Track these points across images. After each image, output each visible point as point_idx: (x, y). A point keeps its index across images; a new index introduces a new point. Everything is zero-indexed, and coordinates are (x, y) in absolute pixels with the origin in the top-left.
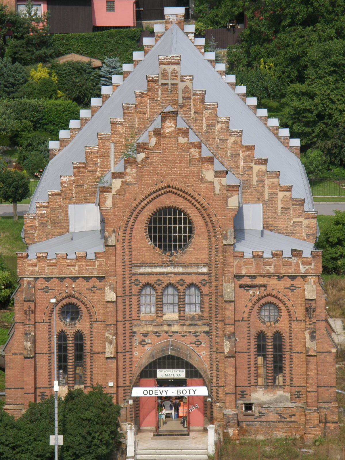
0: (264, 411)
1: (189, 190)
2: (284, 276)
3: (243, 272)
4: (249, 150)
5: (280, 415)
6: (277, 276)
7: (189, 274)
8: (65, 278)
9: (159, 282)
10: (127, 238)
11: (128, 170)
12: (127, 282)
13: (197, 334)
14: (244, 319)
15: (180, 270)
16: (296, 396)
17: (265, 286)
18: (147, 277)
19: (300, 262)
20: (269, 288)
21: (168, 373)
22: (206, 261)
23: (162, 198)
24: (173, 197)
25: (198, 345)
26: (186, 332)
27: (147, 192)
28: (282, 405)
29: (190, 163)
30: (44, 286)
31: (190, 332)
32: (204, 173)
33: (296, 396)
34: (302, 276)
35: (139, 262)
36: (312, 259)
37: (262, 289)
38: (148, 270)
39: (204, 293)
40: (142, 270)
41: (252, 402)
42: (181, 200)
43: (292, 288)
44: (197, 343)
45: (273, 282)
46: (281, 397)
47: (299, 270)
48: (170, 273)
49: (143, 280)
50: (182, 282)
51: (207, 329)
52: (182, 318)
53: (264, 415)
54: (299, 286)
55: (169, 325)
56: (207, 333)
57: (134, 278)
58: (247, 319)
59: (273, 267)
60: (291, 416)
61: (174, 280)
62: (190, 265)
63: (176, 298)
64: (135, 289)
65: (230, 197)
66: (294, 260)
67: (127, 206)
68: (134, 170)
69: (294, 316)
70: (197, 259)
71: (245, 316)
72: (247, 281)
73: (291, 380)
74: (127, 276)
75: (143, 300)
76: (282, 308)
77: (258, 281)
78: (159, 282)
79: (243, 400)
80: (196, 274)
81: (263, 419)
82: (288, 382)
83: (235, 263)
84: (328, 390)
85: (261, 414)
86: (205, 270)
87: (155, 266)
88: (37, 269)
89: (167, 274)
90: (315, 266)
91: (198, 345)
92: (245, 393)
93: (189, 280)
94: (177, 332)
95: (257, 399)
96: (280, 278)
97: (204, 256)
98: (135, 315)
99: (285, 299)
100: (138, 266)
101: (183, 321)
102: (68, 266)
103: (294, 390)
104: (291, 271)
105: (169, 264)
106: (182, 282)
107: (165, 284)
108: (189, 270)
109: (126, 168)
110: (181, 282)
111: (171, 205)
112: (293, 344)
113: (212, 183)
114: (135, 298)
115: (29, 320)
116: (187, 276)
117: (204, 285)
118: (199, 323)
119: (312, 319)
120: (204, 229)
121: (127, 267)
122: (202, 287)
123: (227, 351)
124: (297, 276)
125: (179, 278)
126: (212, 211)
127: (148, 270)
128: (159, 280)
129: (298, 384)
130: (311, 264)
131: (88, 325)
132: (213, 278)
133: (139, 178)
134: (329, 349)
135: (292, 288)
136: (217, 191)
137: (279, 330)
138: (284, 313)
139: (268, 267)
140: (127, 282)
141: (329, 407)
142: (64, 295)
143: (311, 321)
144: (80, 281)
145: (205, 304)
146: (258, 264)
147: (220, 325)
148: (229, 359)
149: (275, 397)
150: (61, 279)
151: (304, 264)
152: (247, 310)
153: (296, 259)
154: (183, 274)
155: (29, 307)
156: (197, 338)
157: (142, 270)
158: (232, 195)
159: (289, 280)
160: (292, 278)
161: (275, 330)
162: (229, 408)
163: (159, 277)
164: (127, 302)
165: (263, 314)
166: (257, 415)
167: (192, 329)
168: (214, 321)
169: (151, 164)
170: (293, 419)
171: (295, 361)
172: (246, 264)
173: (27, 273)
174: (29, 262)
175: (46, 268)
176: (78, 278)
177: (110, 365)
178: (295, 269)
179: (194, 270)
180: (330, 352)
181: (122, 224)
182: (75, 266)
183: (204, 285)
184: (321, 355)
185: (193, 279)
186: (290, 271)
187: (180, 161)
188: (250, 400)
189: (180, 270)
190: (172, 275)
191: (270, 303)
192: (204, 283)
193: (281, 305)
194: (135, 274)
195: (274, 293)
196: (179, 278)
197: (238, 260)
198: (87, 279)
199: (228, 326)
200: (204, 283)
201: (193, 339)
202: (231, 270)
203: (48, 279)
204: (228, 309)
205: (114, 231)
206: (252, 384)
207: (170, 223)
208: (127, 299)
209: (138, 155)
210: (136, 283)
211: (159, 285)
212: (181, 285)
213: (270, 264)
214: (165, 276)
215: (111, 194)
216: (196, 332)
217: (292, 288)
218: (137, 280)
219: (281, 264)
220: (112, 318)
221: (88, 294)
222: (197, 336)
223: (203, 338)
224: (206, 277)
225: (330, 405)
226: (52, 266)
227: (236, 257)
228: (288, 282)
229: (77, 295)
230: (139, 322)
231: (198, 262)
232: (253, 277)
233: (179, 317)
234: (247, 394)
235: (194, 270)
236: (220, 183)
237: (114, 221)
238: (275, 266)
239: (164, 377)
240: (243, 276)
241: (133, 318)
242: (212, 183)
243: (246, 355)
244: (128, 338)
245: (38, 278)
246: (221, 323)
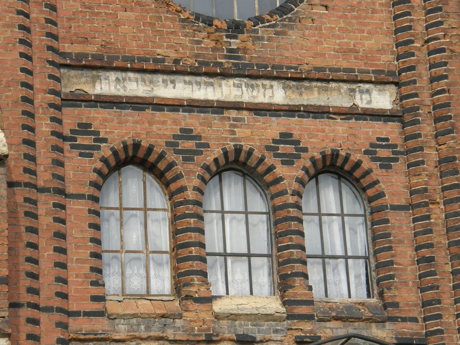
9: (190, 145)
12: (44, 126)
15: (277, 94)
18: (130, 115)
22: (387, 60)
35: (91, 49)
38: (135, 87)
40: (107, 85)
48: (237, 106)
49: (118, 130)
50: (289, 149)
57: (71, 117)
62: (324, 78)
64: (79, 170)
70: (346, 52)
78: (190, 145)
86: (383, 99)
89: (220, 107)
97: (376, 43)
105: (227, 63)
106: (289, 149)
107: (216, 152)
108: (314, 97)
116: (308, 122)
117: (386, 164)
122: (378, 173)
125: (275, 127)
127: (135, 87)
128: (187, 134)
132: (427, 129)
140: (44, 126)
145: (399, 249)
154: (291, 111)
157: (107, 85)
179: (337, 97)
189: (277, 94)
190: (245, 114)
196: (275, 127)
210: (81, 140)
211: (189, 156)
212: (288, 160)
214: (214, 119)
224: (391, 131)
235: (337, 97)
241: (73, 307)
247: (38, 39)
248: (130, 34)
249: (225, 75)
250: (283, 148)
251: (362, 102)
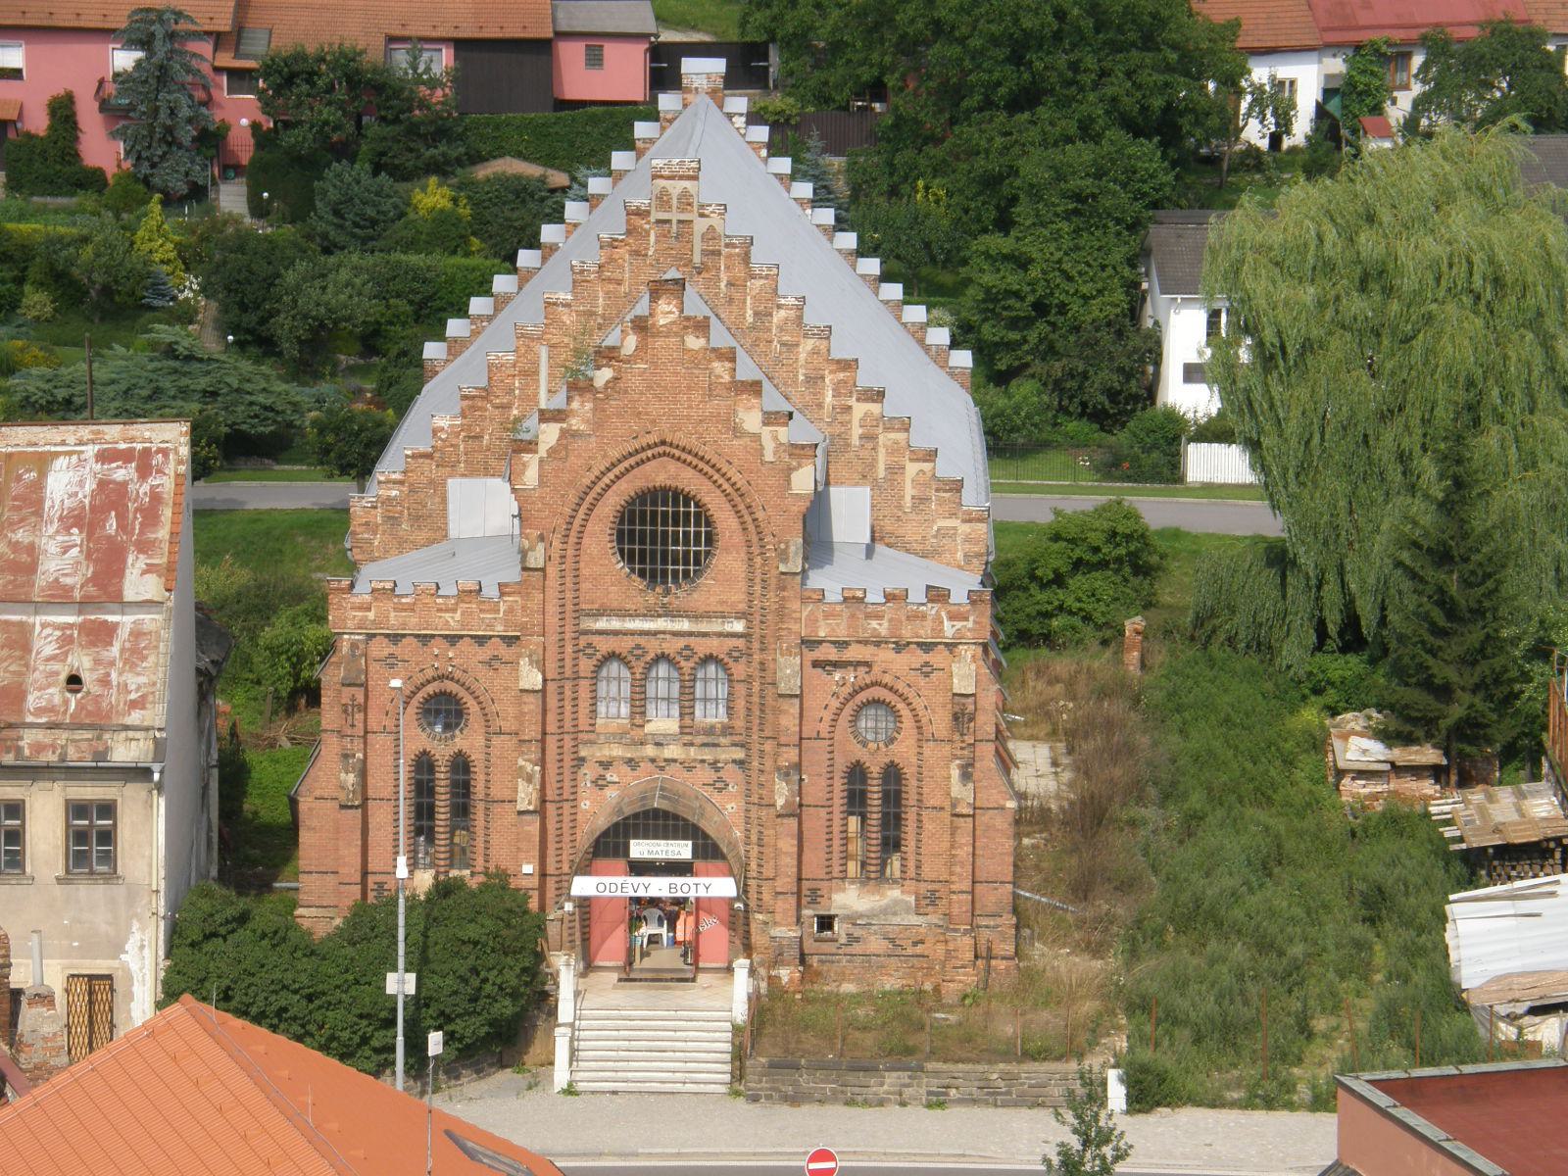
0: (857, 932)
1: (708, 452)
2: (909, 643)
3: (822, 634)
4: (844, 370)
5: (892, 941)
7: (705, 635)
8: (433, 636)
9: (640, 652)
10: (570, 552)
11: (575, 405)
12: (569, 649)
14: (822, 735)
15: (684, 625)
16: (928, 901)
17: (867, 664)
19: (943, 614)
20: (876, 669)
22: (742, 607)
23: (648, 467)
24: (673, 467)
25: (720, 790)
26: (695, 760)
27: (615, 454)
28: (897, 920)
29: (710, 392)
30: (386, 653)
31: (703, 761)
32: (740, 415)
33: (928, 901)
34: (946, 645)
35: (596, 606)
36: (969, 607)
37: (862, 670)
38: (615, 624)
39: (735, 677)
40: (602, 624)
41: (832, 912)
42: (689, 473)
44: (718, 785)
45: (885, 656)
46: (896, 902)
47: (942, 630)
48: (664, 632)
49: (604, 645)
51: (740, 754)
53: (857, 940)
54: (941, 666)
55: (658, 744)
56: (740, 763)
57: (583, 641)
58: (827, 736)
59: (885, 624)
60: (915, 944)
61: (672, 646)
62: (707, 616)
63: (676, 687)
64: (586, 665)
65: (796, 469)
66: (932, 610)
67: (571, 483)
68: (589, 406)
69: (928, 730)
70: (722, 603)
71: (824, 728)
72: (830, 653)
73: (918, 867)
74: (568, 636)
75: (602, 687)
76: (902, 713)
77: (854, 653)
78: (640, 652)
80: (720, 635)
81: (857, 948)
82: (911, 872)
83: (804, 614)
85: (853, 939)
86: (739, 626)
87: (631, 616)
88: (371, 615)
89: (655, 633)
90: (975, 622)
91: (720, 790)
93: (703, 647)
95: (844, 907)
96: (900, 647)
97: (737, 597)
98: (583, 722)
99: (911, 694)
100: (594, 615)
101: (689, 737)
102: (440, 610)
103: (923, 887)
104: (925, 634)
107: (652, 655)
109: (569, 399)
110: (685, 653)
111: (668, 483)
112: (925, 790)
113: (757, 437)
114: (584, 684)
115: (353, 726)
117: (736, 659)
118: (723, 740)
120: (739, 538)
121: (569, 615)
122: (731, 664)
123: (780, 802)
124: (936, 644)
125: (681, 642)
126: (757, 500)
127: (615, 624)
128: (638, 647)
129: (933, 876)
130: (966, 619)
131: (480, 741)
132: (756, 645)
133: (598, 423)
134: (1002, 802)
135: (926, 670)
136: (769, 456)
137: (896, 761)
139: (874, 624)
140: (569, 649)
141: (997, 926)
142: (430, 673)
144: (464, 645)
146: (853, 616)
147: (768, 746)
148: (785, 821)
150: (425, 639)
151: (951, 618)
152: (828, 716)
153: (937, 606)
154: (691, 634)
155: (353, 699)
157: (602, 624)
158: (800, 466)
159: (919, 652)
160: (927, 647)
161: (887, 760)
162: (781, 925)
163: (639, 640)
164: (568, 693)
165: (863, 724)
166: (843, 940)
167: (708, 755)
168: (755, 737)
169: (626, 392)
170: (919, 949)
171: (928, 826)
172: (827, 616)
173: (349, 623)
174: (354, 599)
175: (393, 614)
176: (462, 637)
177: (527, 828)
179: (715, 626)
180: (1003, 808)
181: (560, 522)
182: (454, 611)
183: (736, 659)
185: (713, 646)
186: (922, 632)
187: (689, 388)
189: (684, 625)
190: (668, 636)
191: (876, 702)
192: (735, 654)
193: (901, 706)
194: (586, 632)
195: (887, 679)
196: (681, 642)
197: (810, 607)
198: (481, 640)
199: (784, 749)
200: (736, 655)
201: (709, 775)
202: (795, 627)
203: (395, 638)
204: (786, 712)
205: (542, 538)
207: (665, 523)
208: (568, 685)
209: (598, 373)
211: (638, 658)
212: (687, 658)
213: (879, 617)
215: (537, 456)
216: (716, 762)
217: (926, 670)
218: (589, 645)
219: (903, 618)
220: (533, 727)
221: (483, 673)
222: (717, 770)
223: (731, 774)
224: (740, 643)
225: (999, 921)
226: (405, 610)
227: (805, 600)
228: (919, 657)
229: (458, 674)
230: (592, 736)
232: (842, 645)
233: (681, 727)
235: (715, 626)
236: (776, 438)
237: (543, 515)
238: (890, 620)
239: (646, 856)
240: (820, 642)
242: (757, 437)
243: (823, 812)
244: (567, 772)
245: (374, 635)
246: (769, 742)
247: (569, 607)
250: (685, 653)
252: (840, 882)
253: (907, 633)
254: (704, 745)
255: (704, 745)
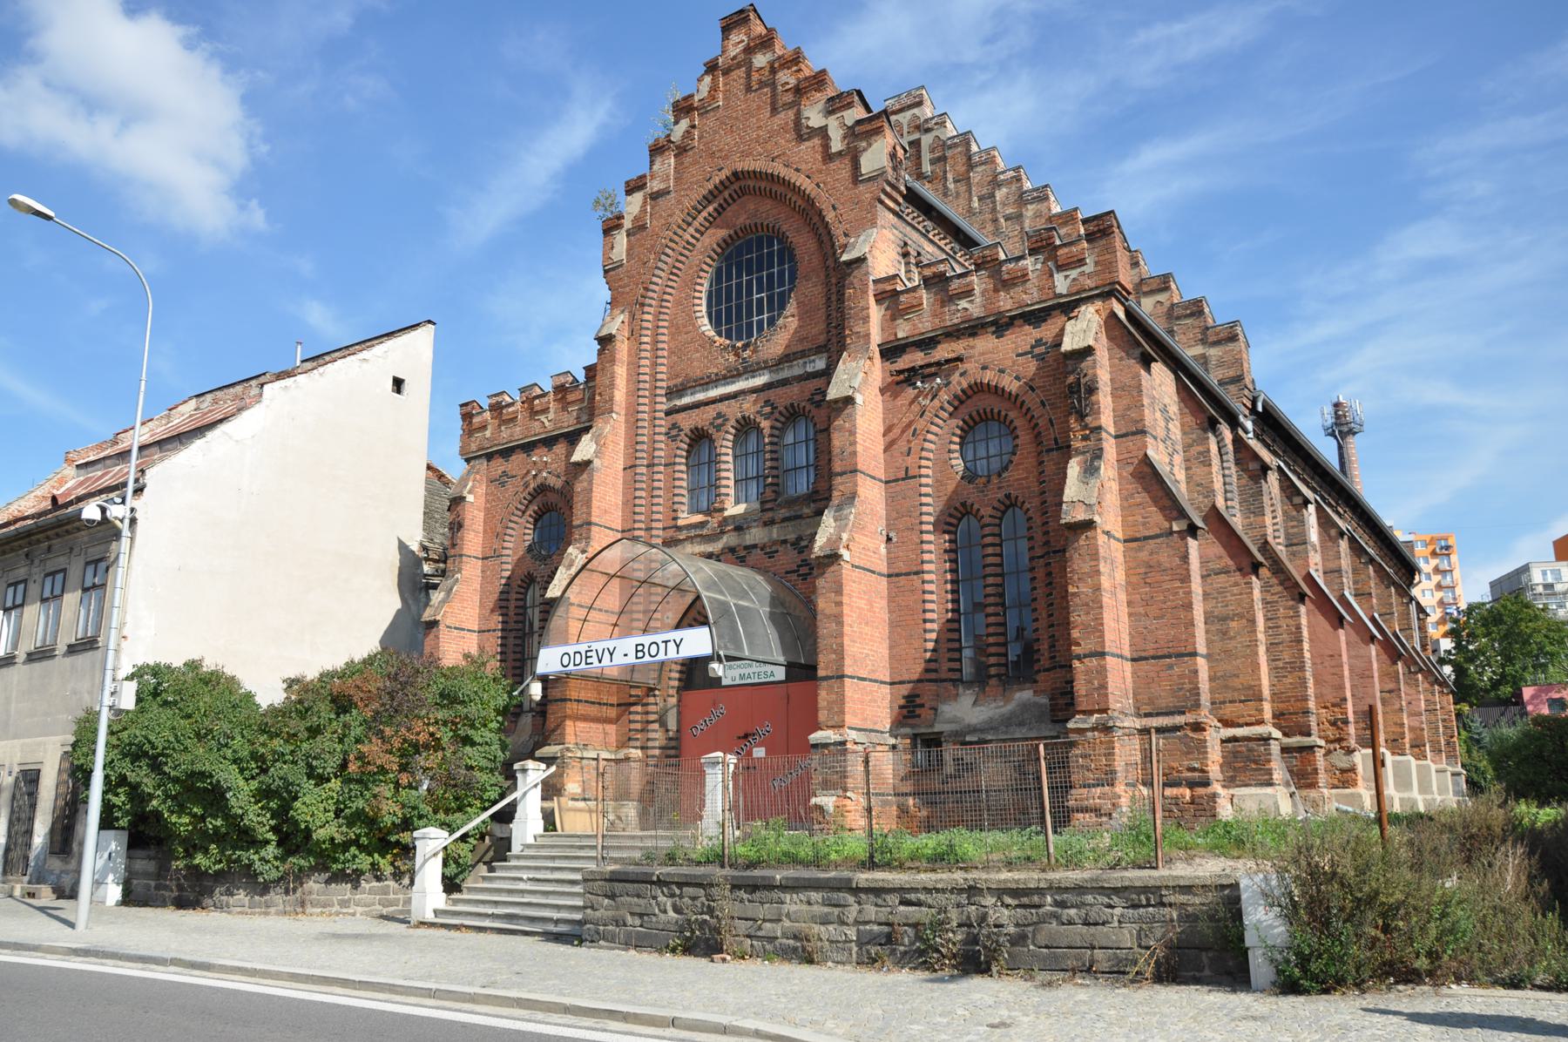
1: (779, 169)
3: (900, 335)
6: (993, 323)
9: (720, 421)
13: (804, 543)
14: (911, 473)
21: (746, 671)
22: (822, 339)
26: (775, 543)
31: (785, 542)
43: (1037, 351)
45: (985, 344)
46: (1025, 707)
48: (742, 392)
52: (768, 506)
72: (916, 358)
77: (943, 352)
78: (720, 421)
79: (912, 726)
84: (1170, 667)
90: (1096, 263)
92: (918, 701)
94: (755, 546)
96: (1000, 325)
104: (1030, 296)
109: (652, 163)
116: (779, 391)
119: (1088, 419)
120: (816, 261)
122: (814, 411)
127: (700, 396)
128: (719, 415)
136: (837, 145)
138: (1024, 437)
139: (963, 304)
143: (1086, 427)
149: (1010, 707)
150: (528, 447)
156: (804, 556)
158: (870, 145)
160: (1035, 317)
161: (1000, 495)
178: (1041, 289)
184: (1140, 549)
188: (932, 726)
195: (988, 377)
206: (944, 676)
211: (718, 428)
213: (968, 293)
216: (800, 539)
228: (1025, 336)
231: (806, 345)
232: (927, 343)
234: (922, 706)
242: (823, 132)
243: (916, 579)
248: (699, 366)
249: (739, 375)
251: (809, 369)
252: (949, 685)
253: (1006, 303)
254: (785, 520)
255: (785, 520)
